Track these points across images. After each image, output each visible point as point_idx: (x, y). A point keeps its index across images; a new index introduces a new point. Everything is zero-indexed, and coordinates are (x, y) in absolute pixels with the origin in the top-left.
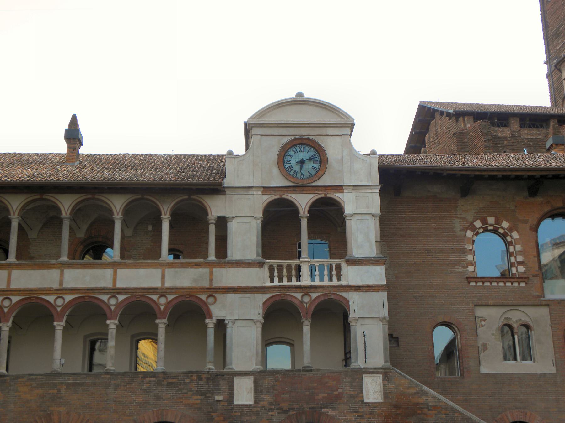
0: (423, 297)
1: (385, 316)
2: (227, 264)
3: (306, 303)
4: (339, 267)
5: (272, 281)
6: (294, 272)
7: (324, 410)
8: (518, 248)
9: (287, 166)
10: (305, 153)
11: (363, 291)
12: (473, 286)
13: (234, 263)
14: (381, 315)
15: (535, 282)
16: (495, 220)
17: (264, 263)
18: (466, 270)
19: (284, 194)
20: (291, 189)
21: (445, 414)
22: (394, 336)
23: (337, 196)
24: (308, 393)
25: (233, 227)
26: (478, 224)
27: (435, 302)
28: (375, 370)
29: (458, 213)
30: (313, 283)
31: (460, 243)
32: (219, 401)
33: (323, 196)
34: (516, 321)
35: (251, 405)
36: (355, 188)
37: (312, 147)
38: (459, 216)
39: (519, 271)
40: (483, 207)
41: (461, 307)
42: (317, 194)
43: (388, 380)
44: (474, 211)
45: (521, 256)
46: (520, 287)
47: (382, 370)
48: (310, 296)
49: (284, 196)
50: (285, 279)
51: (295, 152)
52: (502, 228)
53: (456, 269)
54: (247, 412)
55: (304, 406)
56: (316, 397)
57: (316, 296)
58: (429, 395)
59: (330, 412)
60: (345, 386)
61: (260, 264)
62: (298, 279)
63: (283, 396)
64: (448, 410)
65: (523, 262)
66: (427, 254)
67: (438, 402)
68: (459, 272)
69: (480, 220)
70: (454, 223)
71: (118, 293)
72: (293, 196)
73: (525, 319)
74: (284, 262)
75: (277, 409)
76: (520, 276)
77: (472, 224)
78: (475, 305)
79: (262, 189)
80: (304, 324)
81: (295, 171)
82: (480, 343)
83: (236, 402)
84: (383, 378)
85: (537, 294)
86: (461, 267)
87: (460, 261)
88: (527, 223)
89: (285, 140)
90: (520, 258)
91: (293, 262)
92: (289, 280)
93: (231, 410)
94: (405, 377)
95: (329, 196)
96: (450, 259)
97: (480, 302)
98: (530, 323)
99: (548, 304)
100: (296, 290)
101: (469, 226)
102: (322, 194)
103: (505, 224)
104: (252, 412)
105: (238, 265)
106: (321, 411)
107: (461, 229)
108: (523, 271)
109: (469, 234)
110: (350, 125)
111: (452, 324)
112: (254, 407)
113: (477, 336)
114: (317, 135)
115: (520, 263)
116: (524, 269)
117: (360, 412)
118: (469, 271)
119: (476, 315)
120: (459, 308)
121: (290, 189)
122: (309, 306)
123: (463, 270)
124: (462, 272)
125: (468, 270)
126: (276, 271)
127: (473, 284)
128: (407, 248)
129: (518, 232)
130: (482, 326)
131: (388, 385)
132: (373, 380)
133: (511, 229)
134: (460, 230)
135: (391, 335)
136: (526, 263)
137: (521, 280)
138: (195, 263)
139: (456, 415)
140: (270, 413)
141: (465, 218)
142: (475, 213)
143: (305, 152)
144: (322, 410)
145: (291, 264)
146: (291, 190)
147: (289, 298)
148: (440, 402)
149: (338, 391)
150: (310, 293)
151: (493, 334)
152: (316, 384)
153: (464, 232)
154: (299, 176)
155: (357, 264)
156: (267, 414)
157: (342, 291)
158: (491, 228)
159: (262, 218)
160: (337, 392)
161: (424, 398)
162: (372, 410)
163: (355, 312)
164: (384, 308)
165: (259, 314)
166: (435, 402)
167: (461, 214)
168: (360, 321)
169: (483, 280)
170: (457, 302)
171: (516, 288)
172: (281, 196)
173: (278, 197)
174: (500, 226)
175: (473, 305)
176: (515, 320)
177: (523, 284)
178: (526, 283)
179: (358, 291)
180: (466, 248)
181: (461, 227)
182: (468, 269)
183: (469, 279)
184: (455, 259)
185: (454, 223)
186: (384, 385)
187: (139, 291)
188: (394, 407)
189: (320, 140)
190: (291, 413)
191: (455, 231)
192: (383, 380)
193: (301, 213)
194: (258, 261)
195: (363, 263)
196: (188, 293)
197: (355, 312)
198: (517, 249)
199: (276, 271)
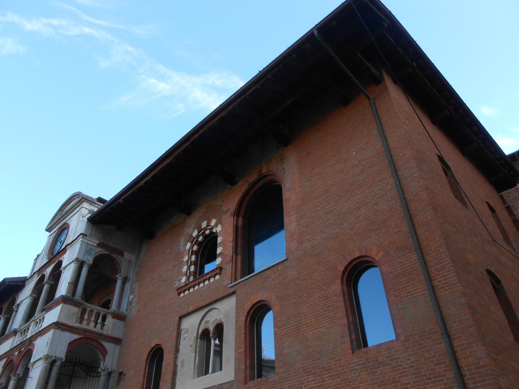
15: (228, 269)
40: (201, 216)
44: (194, 223)
79: (37, 274)
80: (12, 379)
97: (185, 312)
116: (221, 259)
127: (182, 295)
155: (50, 310)
159: (30, 295)
167: (186, 232)
169: (187, 287)
171: (212, 284)
173: (41, 275)
176: (212, 322)
177: (218, 277)
178: (220, 274)
179: (41, 335)
181: (184, 242)
195: (52, 307)
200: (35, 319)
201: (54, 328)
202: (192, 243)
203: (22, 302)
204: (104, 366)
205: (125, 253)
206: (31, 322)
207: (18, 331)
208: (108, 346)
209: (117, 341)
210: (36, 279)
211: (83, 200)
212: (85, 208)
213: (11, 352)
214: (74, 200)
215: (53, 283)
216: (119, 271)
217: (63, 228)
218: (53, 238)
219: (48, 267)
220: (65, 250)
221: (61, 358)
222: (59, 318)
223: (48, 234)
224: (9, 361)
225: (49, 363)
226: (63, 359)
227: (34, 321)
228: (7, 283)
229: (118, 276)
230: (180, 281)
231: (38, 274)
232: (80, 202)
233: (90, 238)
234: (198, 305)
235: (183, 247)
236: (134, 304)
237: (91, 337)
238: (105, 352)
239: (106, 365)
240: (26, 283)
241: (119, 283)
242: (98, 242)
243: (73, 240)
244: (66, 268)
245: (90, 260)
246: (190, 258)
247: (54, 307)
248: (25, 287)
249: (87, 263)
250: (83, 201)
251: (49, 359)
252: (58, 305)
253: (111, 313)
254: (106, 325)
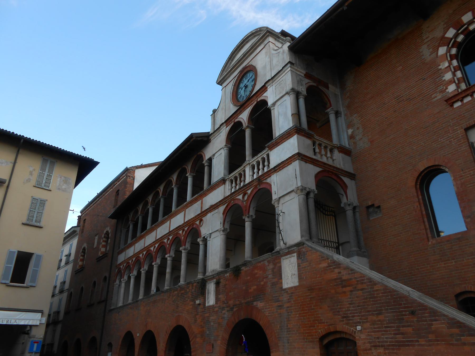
0: (400, 149)
1: (298, 186)
2: (208, 191)
7: (255, 303)
11: (280, 169)
12: (458, 107)
13: (210, 189)
14: (294, 187)
18: (446, 93)
21: (362, 290)
22: (376, 205)
24: (244, 288)
25: (214, 162)
27: (414, 149)
28: (290, 250)
31: (432, 68)
32: (199, 304)
35: (213, 306)
36: (274, 80)
38: (425, 41)
41: (446, 141)
43: (302, 258)
47: (296, 248)
53: (435, 98)
54: (212, 312)
55: (243, 301)
56: (250, 291)
57: (250, 192)
58: (342, 266)
59: (260, 304)
60: (269, 274)
61: (221, 182)
63: (230, 294)
64: (365, 283)
66: (396, 102)
67: (352, 273)
68: (437, 100)
70: (422, 52)
71: (170, 235)
75: (227, 307)
79: (225, 124)
81: (243, 96)
83: (207, 305)
84: (297, 257)
86: (438, 94)
87: (435, 88)
93: (204, 311)
94: (317, 251)
95: (259, 100)
96: (424, 92)
100: (239, 193)
101: (440, 42)
104: (214, 312)
105: (212, 190)
106: (253, 305)
109: (442, 50)
110: (268, 34)
111: (441, 166)
112: (215, 307)
114: (252, 60)
117: (279, 301)
118: (450, 91)
120: (444, 142)
121: (238, 113)
123: (442, 96)
124: (440, 99)
125: (448, 92)
128: (377, 108)
131: (302, 263)
132: (290, 261)
134: (430, 54)
138: (195, 199)
139: (376, 288)
140: (223, 312)
141: (434, 38)
142: (444, 25)
144: (253, 304)
145: (240, 172)
146: (238, 112)
148: (354, 273)
149: (263, 281)
152: (249, 278)
153: (434, 55)
155: (276, 146)
156: (222, 312)
157: (266, 177)
159: (225, 146)
160: (263, 282)
161: (337, 271)
162: (290, 296)
163: (275, 194)
164: (296, 178)
166: (349, 274)
167: (427, 38)
168: (282, 201)
170: (439, 137)
173: (233, 123)
175: (463, 130)
179: (277, 171)
180: (441, 69)
181: (431, 50)
182: (447, 90)
183: (450, 101)
184: (431, 88)
185: (422, 52)
186: (299, 266)
187: (175, 231)
188: (309, 290)
190: (235, 309)
191: (424, 59)
192: (298, 259)
194: (219, 180)
195: (279, 142)
196: (192, 223)
197: (275, 194)
200: (249, 162)
201: (299, 159)
202: (448, 46)
203: (214, 155)
204: (347, 200)
205: (330, 86)
206: (245, 167)
207: (226, 180)
208: (346, 180)
209: (352, 176)
210: (225, 131)
211: (268, 34)
212: (272, 43)
213: (230, 197)
214: (247, 42)
215: (254, 127)
216: (329, 105)
217: (244, 73)
218: (233, 86)
219: (241, 113)
220: (265, 88)
221: (314, 190)
222: (299, 149)
223: (220, 87)
224: (229, 207)
225: (305, 195)
226: (315, 191)
227: (248, 165)
228: (194, 138)
229: (329, 110)
230: (443, 91)
231: (226, 125)
232: (263, 39)
233: (298, 68)
235: (430, 55)
236: (357, 138)
237: (330, 170)
238: (345, 187)
239: (350, 200)
240: (210, 138)
241: (332, 117)
242: (304, 72)
243: (273, 76)
244: (275, 104)
245: (303, 90)
246: (450, 64)
247: (283, 141)
248: (211, 142)
249: (302, 94)
250: (268, 36)
251: (304, 191)
252: (291, 137)
253: (337, 147)
254: (336, 159)
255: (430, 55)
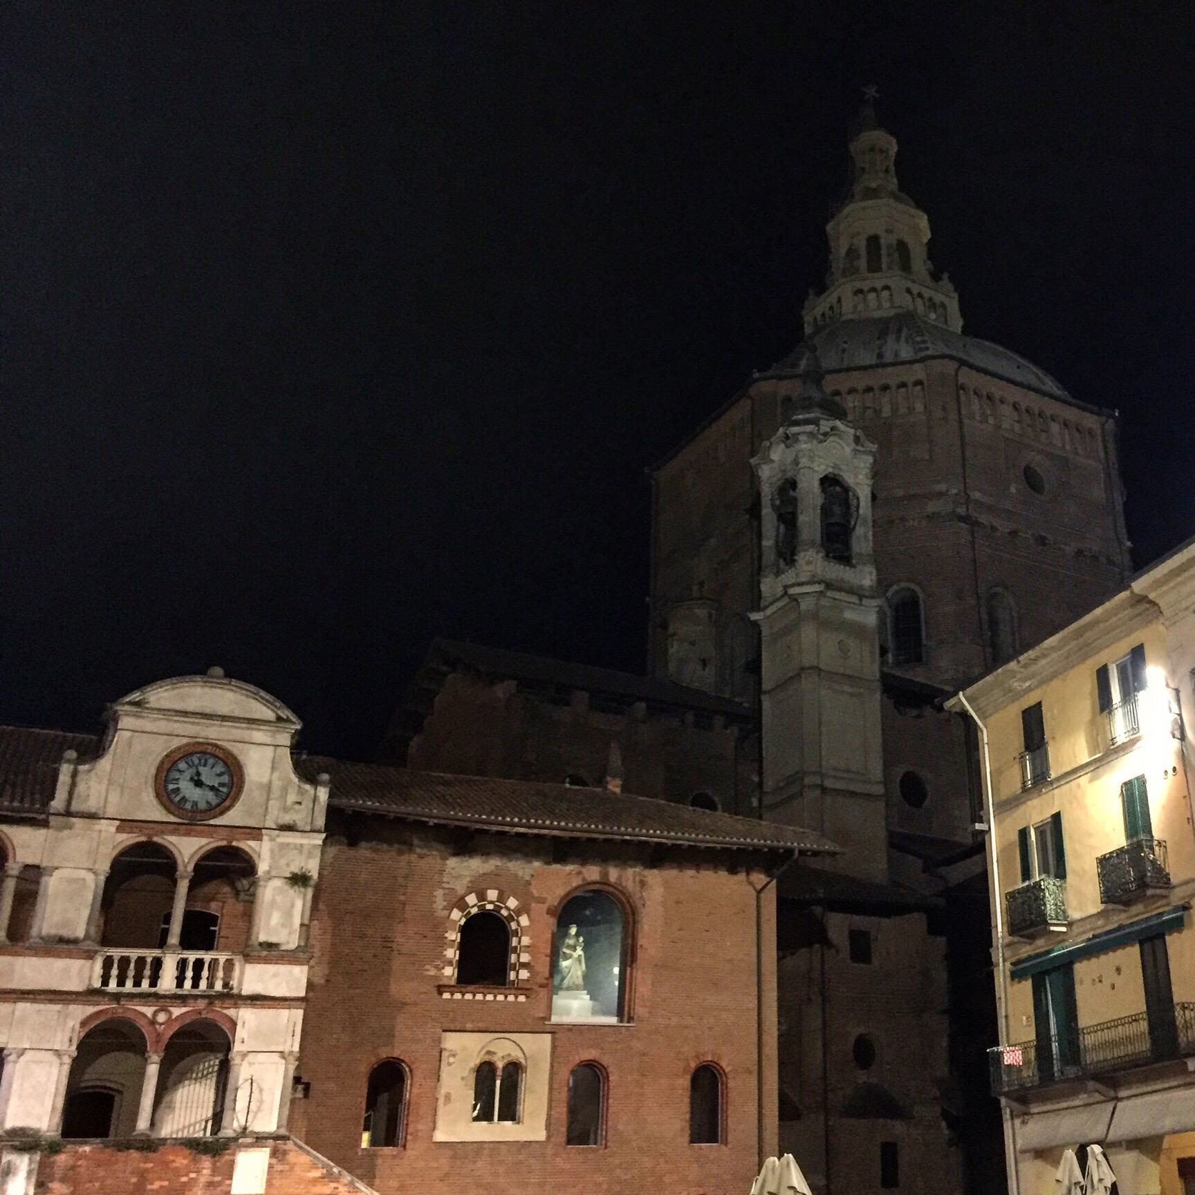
3: (161, 1024)
4: (229, 965)
5: (105, 982)
6: (147, 972)
8: (526, 940)
9: (171, 787)
10: (206, 768)
16: (499, 894)
17: (96, 952)
19: (157, 836)
20: (171, 827)
23: (249, 845)
26: (471, 899)
29: (445, 879)
30: (179, 992)
33: (224, 843)
34: (503, 1057)
37: (222, 760)
39: (521, 977)
42: (212, 840)
44: (468, 879)
45: (527, 954)
46: (516, 1003)
48: (170, 1013)
49: (155, 839)
50: (129, 984)
51: (188, 764)
52: (508, 908)
53: (427, 970)
62: (153, 983)
65: (529, 963)
68: (430, 976)
69: (476, 894)
72: (173, 839)
73: (516, 1054)
74: (134, 954)
76: (520, 985)
77: (462, 898)
78: (444, 1031)
82: (443, 1091)
85: (542, 1015)
88: (544, 903)
89: (176, 743)
90: (525, 958)
91: (150, 954)
92: (137, 983)
95: (234, 844)
98: (523, 1061)
99: (555, 1031)
102: (223, 839)
103: (512, 903)
107: (445, 906)
108: (525, 978)
113: (439, 1081)
115: (525, 966)
116: (528, 975)
118: (446, 974)
119: (443, 1046)
122: (164, 1028)
126: (115, 966)
127: (446, 996)
129: (529, 916)
130: (450, 1064)
133: (519, 912)
135: (297, 1080)
136: (532, 964)
137: (520, 992)
141: (453, 889)
142: (470, 882)
143: (209, 766)
145: (144, 955)
147: (129, 1015)
150: (171, 1009)
151: (463, 1079)
153: (446, 912)
154: (188, 806)
158: (489, 907)
165: (71, 1041)
167: (448, 883)
172: (150, 836)
173: (143, 839)
174: (505, 904)
177: (522, 999)
178: (527, 997)
180: (446, 938)
181: (445, 903)
182: (443, 971)
185: (436, 897)
189: (235, 749)
193: (180, 867)
198: (522, 944)
199: (115, 966)
234: (481, 1025)
235: (443, 909)
255: (443, 909)
